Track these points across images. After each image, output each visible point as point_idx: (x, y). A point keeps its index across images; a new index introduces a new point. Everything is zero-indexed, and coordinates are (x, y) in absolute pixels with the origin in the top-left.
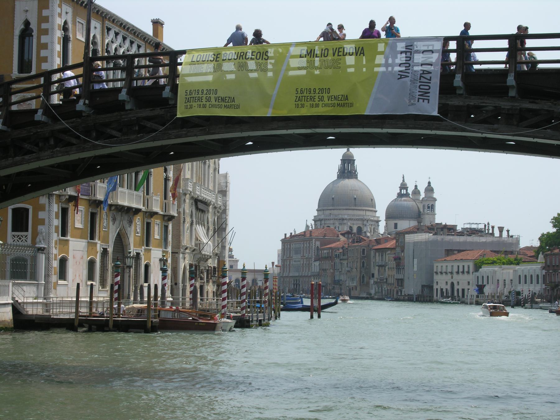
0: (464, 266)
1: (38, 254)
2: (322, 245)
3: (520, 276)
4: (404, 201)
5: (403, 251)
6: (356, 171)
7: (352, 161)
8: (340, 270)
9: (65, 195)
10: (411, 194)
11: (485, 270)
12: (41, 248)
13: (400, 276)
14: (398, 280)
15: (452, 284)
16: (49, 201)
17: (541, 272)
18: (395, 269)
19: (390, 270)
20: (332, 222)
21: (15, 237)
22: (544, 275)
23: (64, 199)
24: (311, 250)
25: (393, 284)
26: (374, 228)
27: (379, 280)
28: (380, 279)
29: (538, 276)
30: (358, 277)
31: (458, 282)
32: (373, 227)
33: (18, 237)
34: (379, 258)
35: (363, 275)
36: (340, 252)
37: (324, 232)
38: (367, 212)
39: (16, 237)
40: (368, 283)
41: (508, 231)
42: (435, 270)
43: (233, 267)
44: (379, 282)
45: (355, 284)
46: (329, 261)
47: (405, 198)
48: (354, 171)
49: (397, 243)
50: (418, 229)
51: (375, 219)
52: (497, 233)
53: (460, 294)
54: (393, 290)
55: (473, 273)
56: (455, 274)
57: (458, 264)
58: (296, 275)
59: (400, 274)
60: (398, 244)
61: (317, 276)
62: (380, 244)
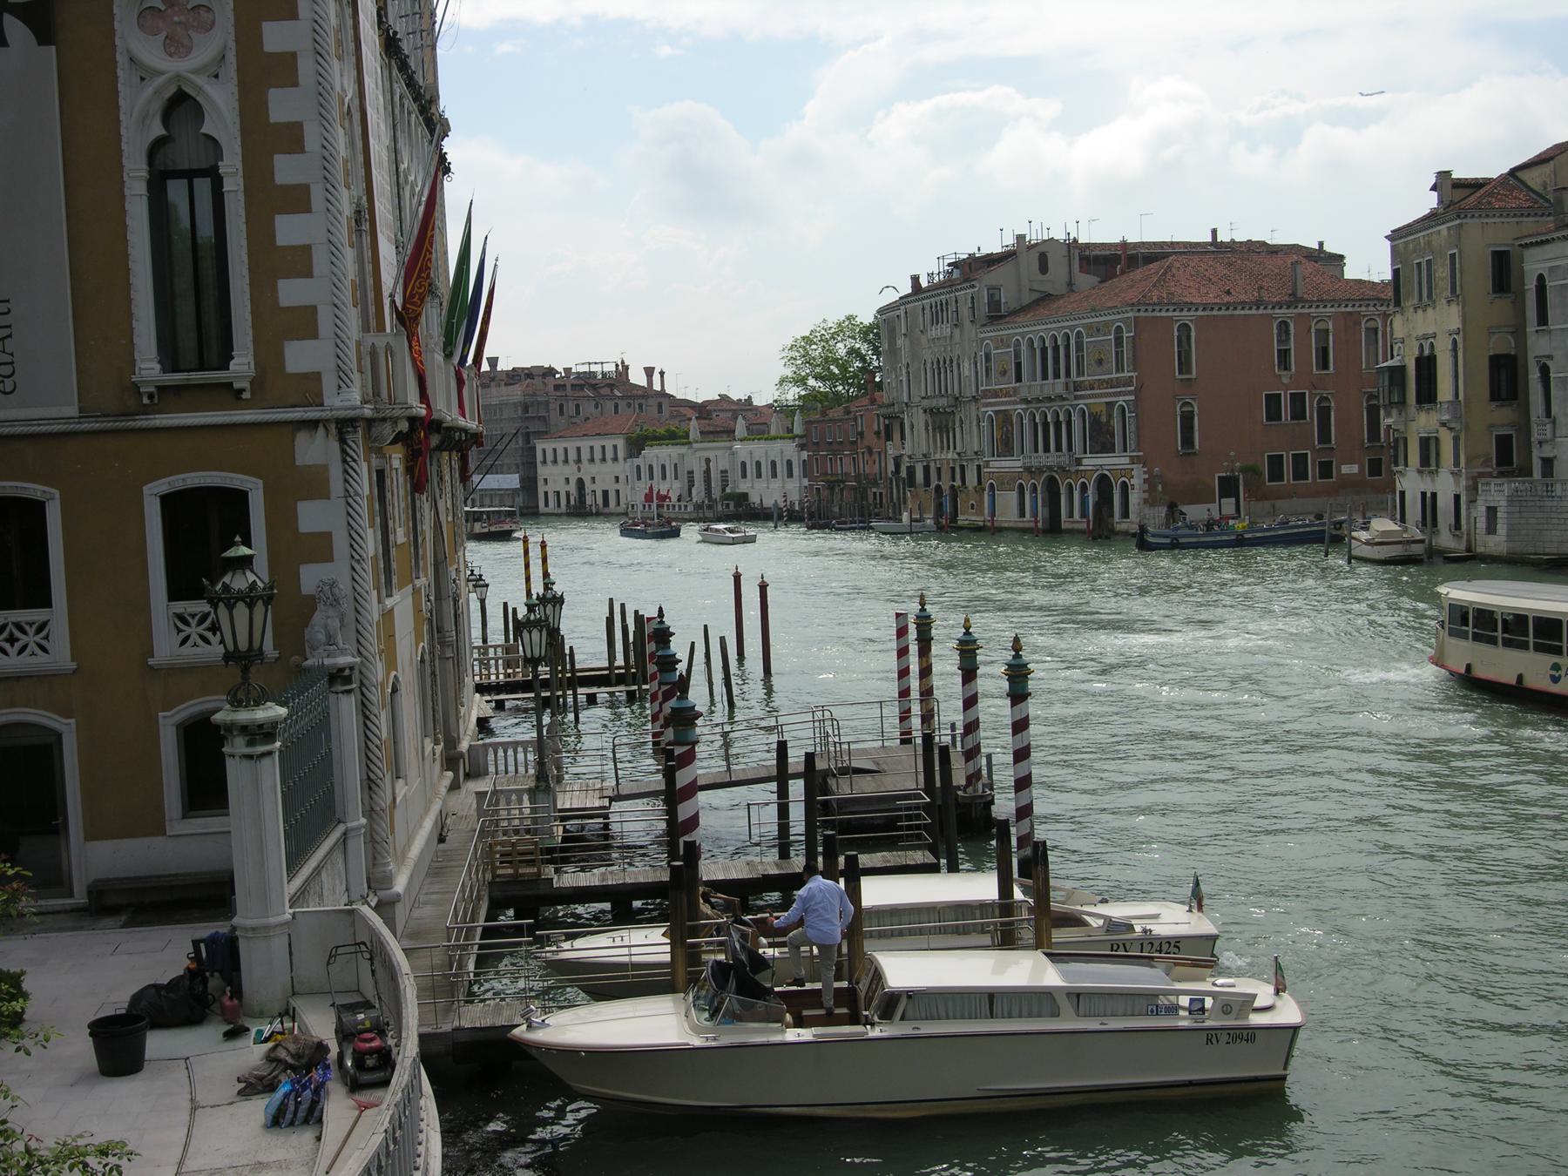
0: (603, 447)
1: (332, 697)
3: (744, 464)
9: (395, 421)
11: (655, 454)
12: (342, 670)
15: (580, 483)
16: (344, 451)
17: (799, 456)
21: (187, 623)
22: (804, 461)
23: (388, 432)
29: (789, 463)
33: (201, 622)
39: (193, 622)
41: (662, 374)
42: (539, 457)
50: (493, 379)
52: (637, 378)
53: (600, 501)
55: (625, 459)
57: (591, 443)
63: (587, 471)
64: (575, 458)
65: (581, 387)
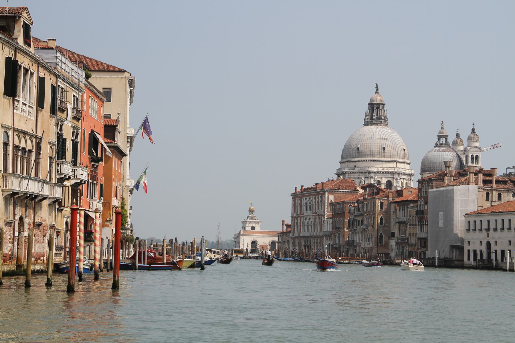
0: (503, 220)
2: (335, 198)
4: (443, 151)
5: (426, 203)
6: (385, 117)
7: (381, 106)
8: (355, 229)
10: (451, 143)
13: (423, 235)
14: (420, 239)
15: (489, 244)
18: (418, 227)
19: (412, 228)
20: (356, 175)
24: (323, 205)
25: (416, 245)
26: (406, 183)
27: (400, 241)
28: (401, 239)
30: (375, 236)
31: (496, 242)
32: (405, 181)
34: (400, 212)
35: (381, 234)
36: (355, 207)
37: (340, 184)
38: (398, 164)
40: (387, 244)
43: (255, 229)
44: (400, 243)
45: (371, 245)
46: (343, 218)
47: (444, 148)
48: (383, 118)
49: (420, 194)
51: (408, 172)
54: (415, 252)
56: (491, 230)
57: (496, 218)
58: (307, 236)
59: (423, 231)
60: (421, 195)
61: (329, 236)
62: (402, 196)
63: (494, 236)
64: (487, 227)
65: (505, 182)
